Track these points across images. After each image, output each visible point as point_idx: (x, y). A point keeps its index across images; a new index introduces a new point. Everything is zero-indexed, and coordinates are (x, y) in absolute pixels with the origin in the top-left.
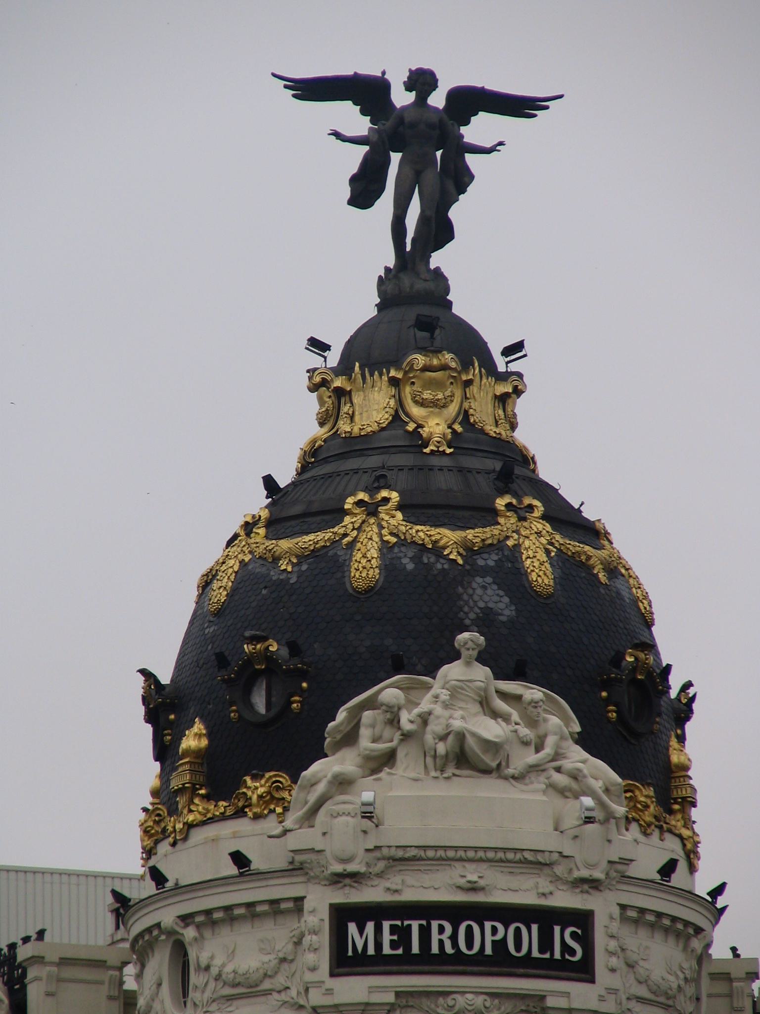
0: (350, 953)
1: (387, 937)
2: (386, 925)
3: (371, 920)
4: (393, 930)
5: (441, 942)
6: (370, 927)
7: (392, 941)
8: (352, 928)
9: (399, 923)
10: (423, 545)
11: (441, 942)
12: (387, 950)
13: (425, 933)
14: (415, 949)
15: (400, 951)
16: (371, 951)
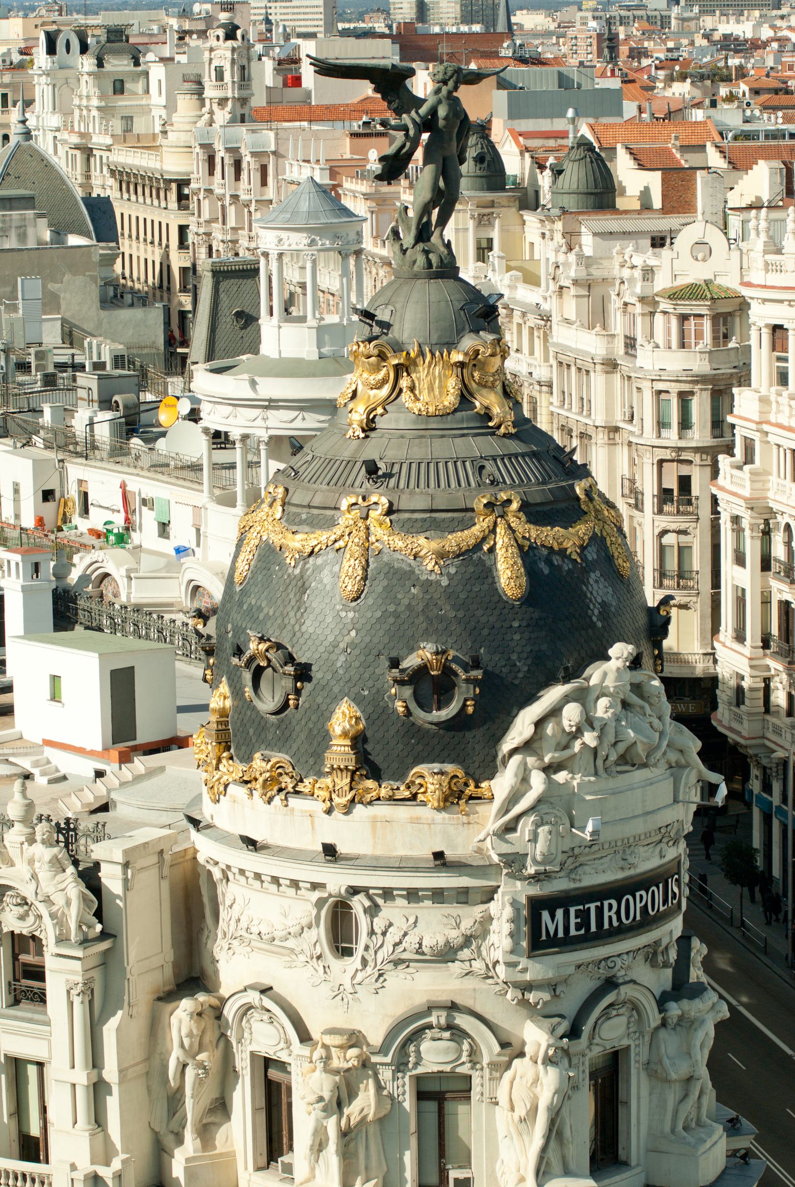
0: (544, 937)
1: (573, 921)
2: (572, 910)
3: (560, 907)
4: (578, 914)
5: (610, 918)
6: (560, 913)
7: (576, 924)
8: (545, 915)
9: (581, 907)
10: (551, 547)
11: (610, 918)
12: (573, 932)
13: (600, 911)
14: (593, 928)
15: (582, 932)
16: (561, 934)
